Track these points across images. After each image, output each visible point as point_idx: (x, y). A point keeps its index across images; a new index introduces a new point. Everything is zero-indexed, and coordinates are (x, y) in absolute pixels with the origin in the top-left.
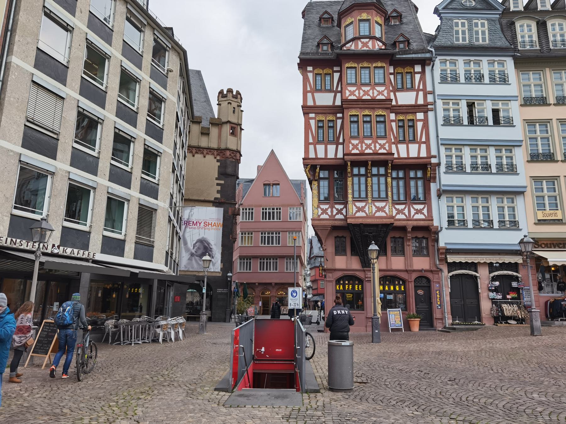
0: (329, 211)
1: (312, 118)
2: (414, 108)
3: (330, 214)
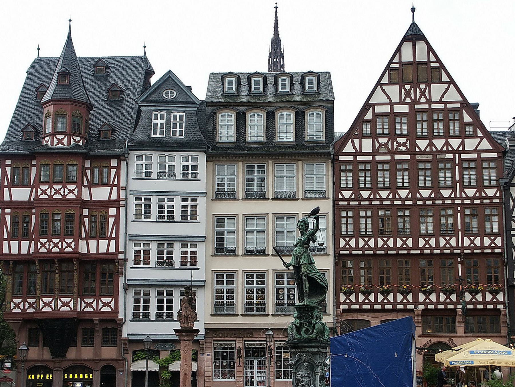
0: (21, 306)
3: (22, 308)
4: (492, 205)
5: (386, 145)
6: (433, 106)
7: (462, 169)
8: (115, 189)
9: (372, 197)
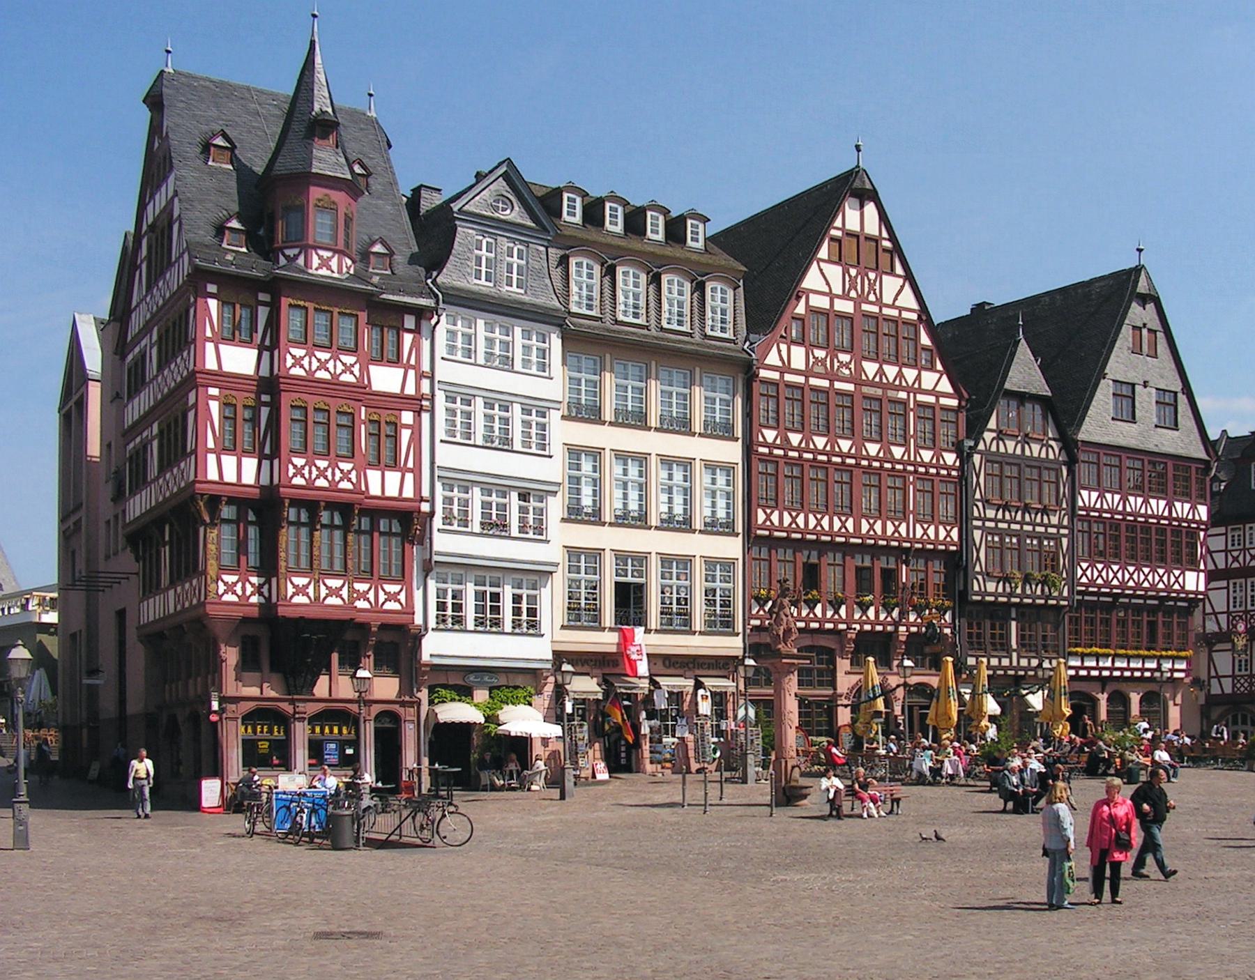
1: (213, 398)
2: (402, 401)
5: (823, 361)
6: (886, 311)
7: (918, 418)
8: (411, 373)
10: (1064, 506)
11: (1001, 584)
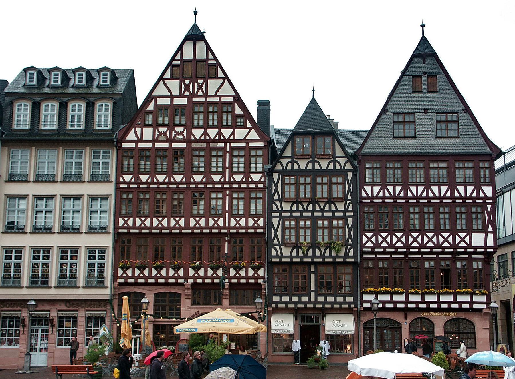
4: (257, 190)
5: (165, 133)
6: (209, 99)
7: (232, 157)
9: (150, 181)
10: (349, 197)
11: (295, 250)
